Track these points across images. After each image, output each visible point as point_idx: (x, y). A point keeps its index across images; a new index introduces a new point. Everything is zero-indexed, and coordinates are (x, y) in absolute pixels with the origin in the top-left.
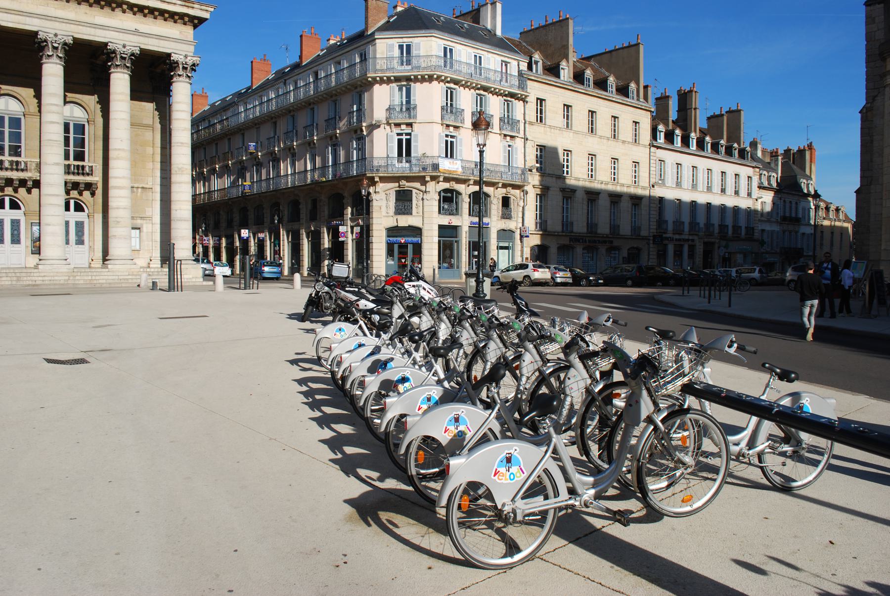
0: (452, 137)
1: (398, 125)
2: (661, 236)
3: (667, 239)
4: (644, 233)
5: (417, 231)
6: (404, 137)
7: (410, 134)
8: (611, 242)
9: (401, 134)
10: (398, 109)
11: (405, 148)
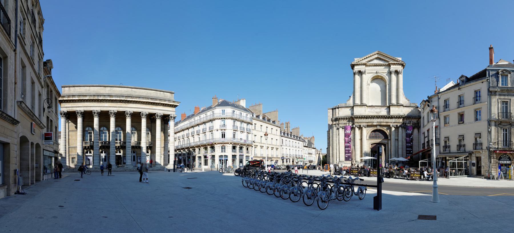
0: (235, 133)
1: (222, 130)
2: (283, 158)
3: (284, 158)
4: (279, 157)
5: (226, 156)
6: (223, 133)
7: (225, 132)
8: (272, 159)
9: (223, 132)
10: (222, 126)
11: (223, 136)
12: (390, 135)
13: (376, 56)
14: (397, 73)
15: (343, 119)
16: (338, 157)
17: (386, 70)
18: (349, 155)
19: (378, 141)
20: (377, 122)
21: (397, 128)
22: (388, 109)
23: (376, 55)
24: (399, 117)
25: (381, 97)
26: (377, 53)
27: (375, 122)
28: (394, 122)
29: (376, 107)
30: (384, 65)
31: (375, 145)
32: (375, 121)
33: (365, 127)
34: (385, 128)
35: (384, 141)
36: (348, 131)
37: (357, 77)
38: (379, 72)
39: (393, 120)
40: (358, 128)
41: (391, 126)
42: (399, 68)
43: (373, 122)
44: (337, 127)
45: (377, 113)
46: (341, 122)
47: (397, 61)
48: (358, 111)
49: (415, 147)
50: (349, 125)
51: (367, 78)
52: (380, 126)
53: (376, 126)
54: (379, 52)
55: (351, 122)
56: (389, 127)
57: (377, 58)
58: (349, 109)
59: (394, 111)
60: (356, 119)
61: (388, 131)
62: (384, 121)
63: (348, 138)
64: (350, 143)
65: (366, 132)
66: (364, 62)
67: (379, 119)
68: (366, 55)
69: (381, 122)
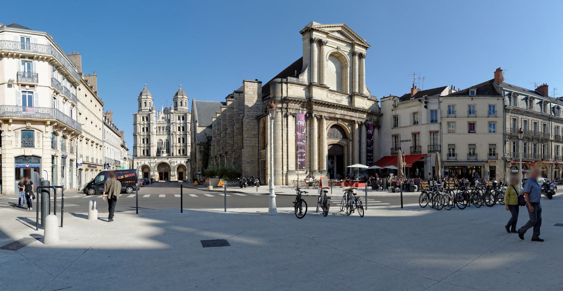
12: (353, 133)
13: (340, 29)
14: (361, 56)
15: (296, 101)
16: (285, 163)
17: (348, 49)
18: (301, 160)
19: (336, 141)
20: (341, 114)
21: (360, 125)
22: (350, 98)
23: (340, 28)
24: (362, 111)
25: (337, 81)
26: (342, 26)
27: (339, 114)
28: (358, 118)
29: (336, 93)
30: (346, 42)
31: (332, 146)
32: (339, 113)
33: (326, 119)
34: (347, 124)
35: (343, 142)
36: (302, 123)
37: (315, 45)
38: (341, 49)
39: (357, 115)
40: (317, 118)
41: (356, 122)
42: (363, 51)
43: (336, 114)
44: (284, 113)
45: (337, 100)
46: (291, 105)
47: (363, 43)
48: (318, 94)
49: (375, 152)
50: (302, 113)
51: (327, 50)
52: (344, 120)
53: (337, 119)
54: (346, 25)
55: (305, 109)
56: (352, 123)
57: (338, 32)
58: (303, 88)
59: (360, 103)
60: (315, 106)
61: (350, 128)
62: (349, 115)
63: (302, 133)
64: (304, 141)
65: (326, 124)
66: (327, 30)
67: (342, 111)
68: (330, 24)
69: (345, 115)
